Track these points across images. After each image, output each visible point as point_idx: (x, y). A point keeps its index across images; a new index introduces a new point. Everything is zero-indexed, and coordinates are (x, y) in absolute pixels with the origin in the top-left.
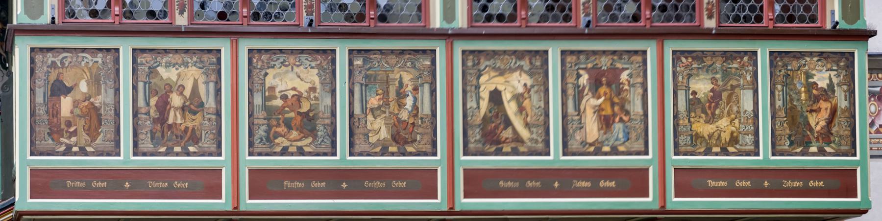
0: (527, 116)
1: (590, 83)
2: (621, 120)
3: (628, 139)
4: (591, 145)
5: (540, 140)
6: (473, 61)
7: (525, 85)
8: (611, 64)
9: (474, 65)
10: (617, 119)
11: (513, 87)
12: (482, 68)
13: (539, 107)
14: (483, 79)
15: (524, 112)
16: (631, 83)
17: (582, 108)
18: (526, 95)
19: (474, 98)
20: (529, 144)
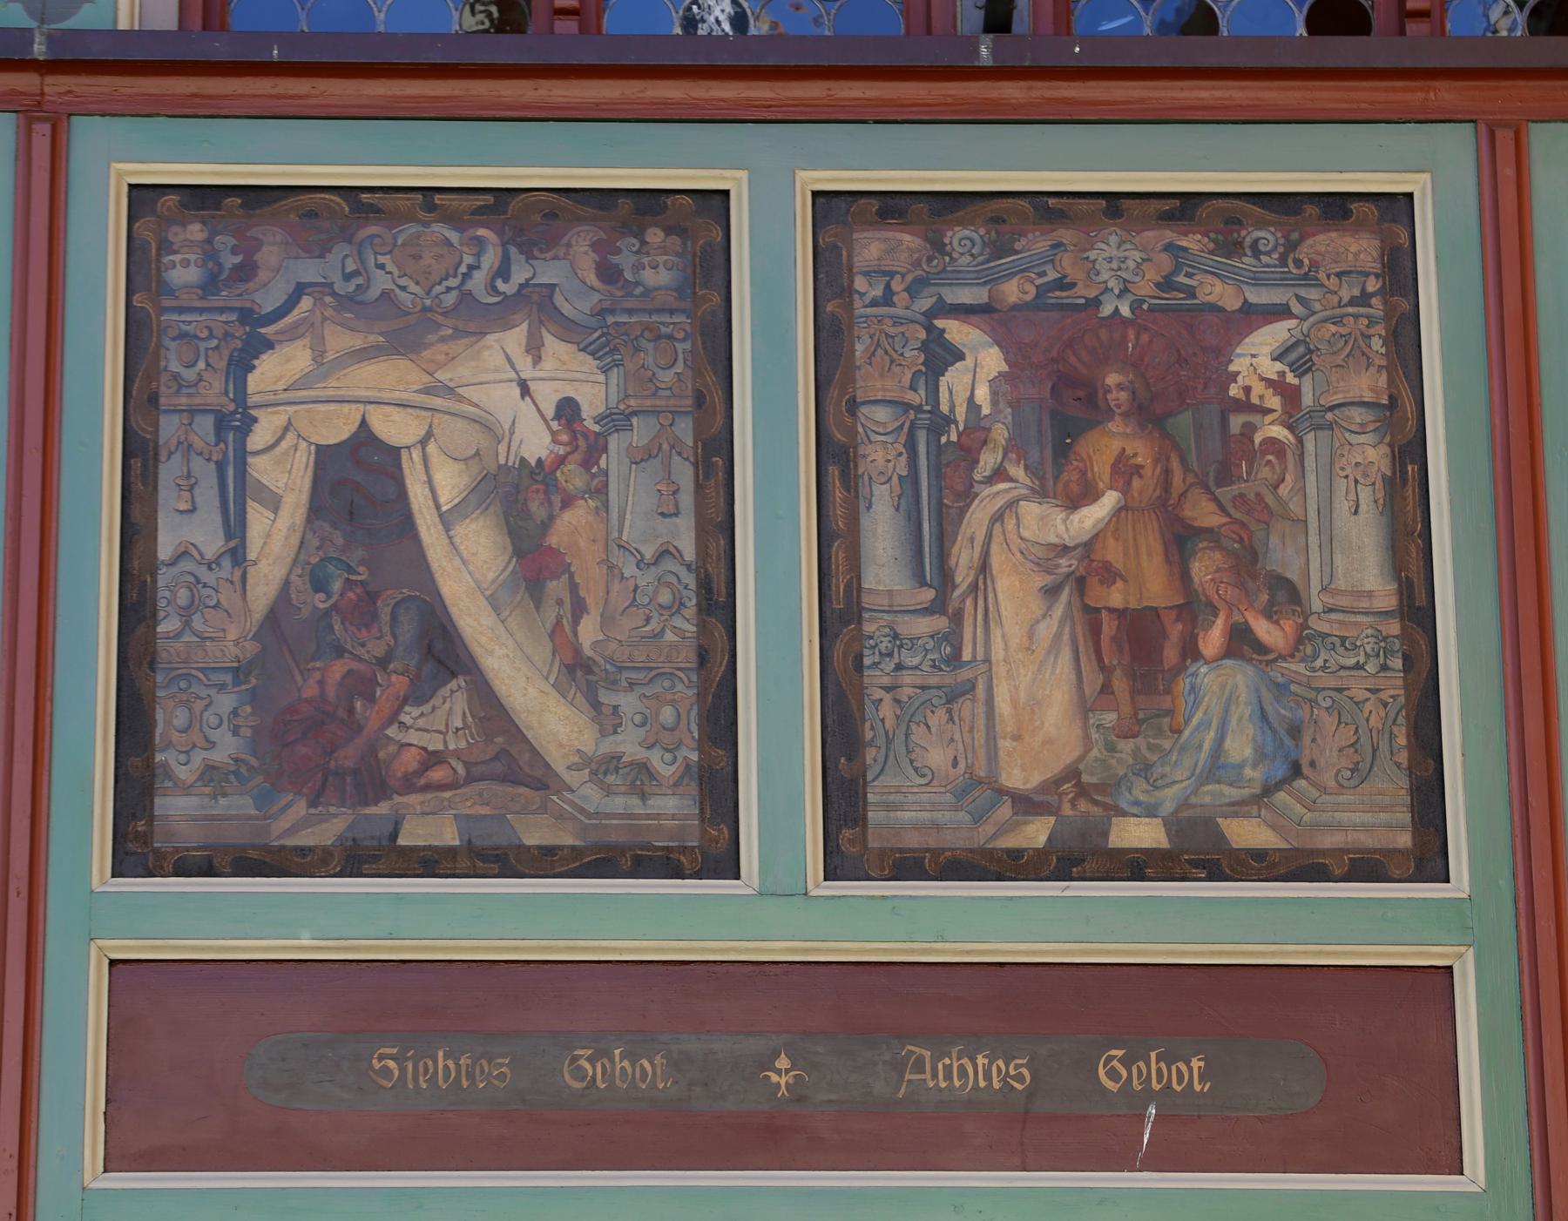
0: (579, 609)
1: (1015, 405)
2: (1241, 643)
3: (1296, 771)
4: (1027, 805)
5: (666, 770)
6: (210, 254)
7: (567, 410)
8: (1166, 284)
9: (211, 285)
10: (1213, 639)
11: (486, 425)
12: (269, 301)
13: (664, 553)
14: (268, 373)
15: (556, 587)
16: (1307, 400)
17: (963, 560)
18: (572, 477)
19: (207, 495)
20: (591, 796)
